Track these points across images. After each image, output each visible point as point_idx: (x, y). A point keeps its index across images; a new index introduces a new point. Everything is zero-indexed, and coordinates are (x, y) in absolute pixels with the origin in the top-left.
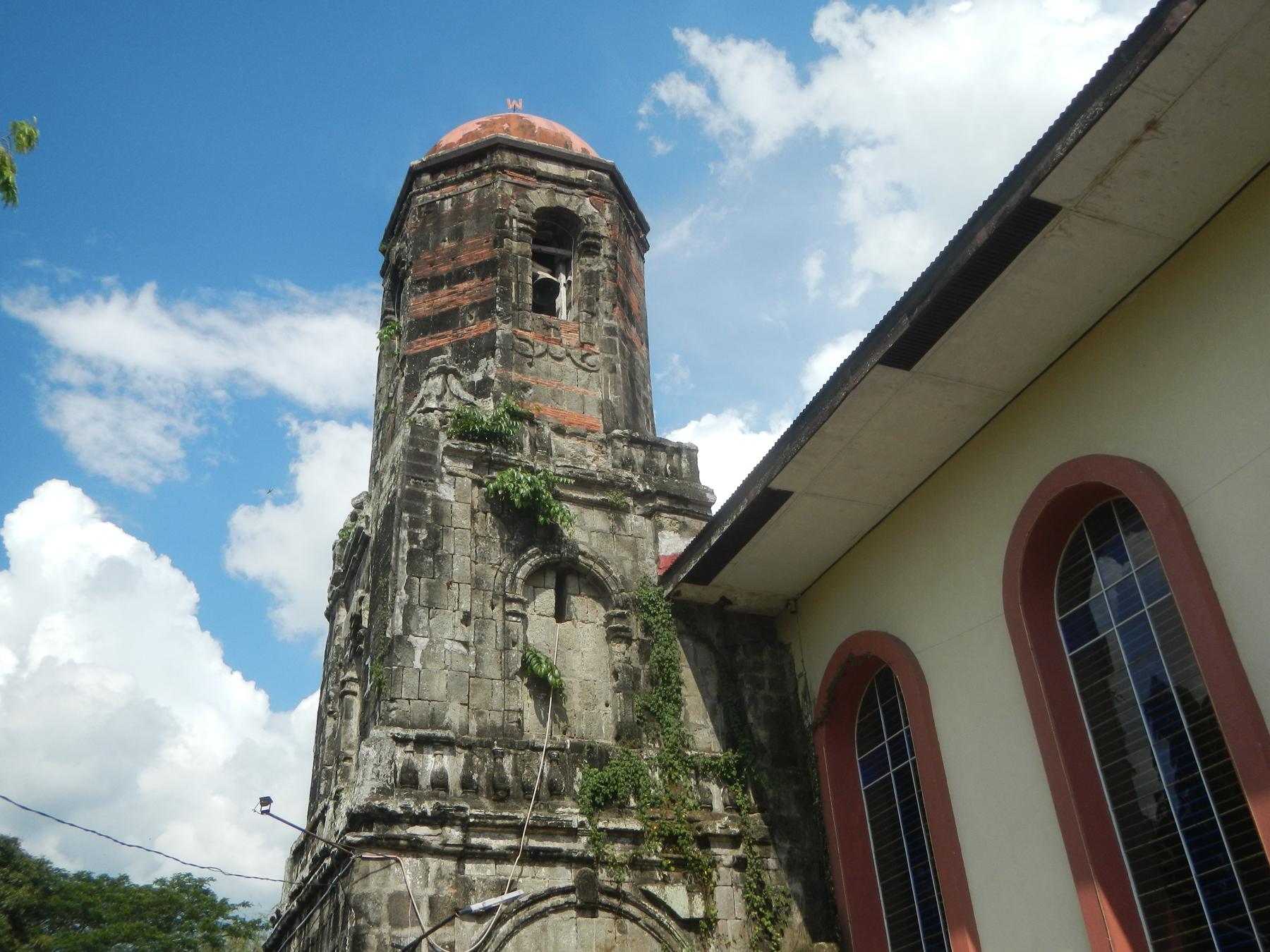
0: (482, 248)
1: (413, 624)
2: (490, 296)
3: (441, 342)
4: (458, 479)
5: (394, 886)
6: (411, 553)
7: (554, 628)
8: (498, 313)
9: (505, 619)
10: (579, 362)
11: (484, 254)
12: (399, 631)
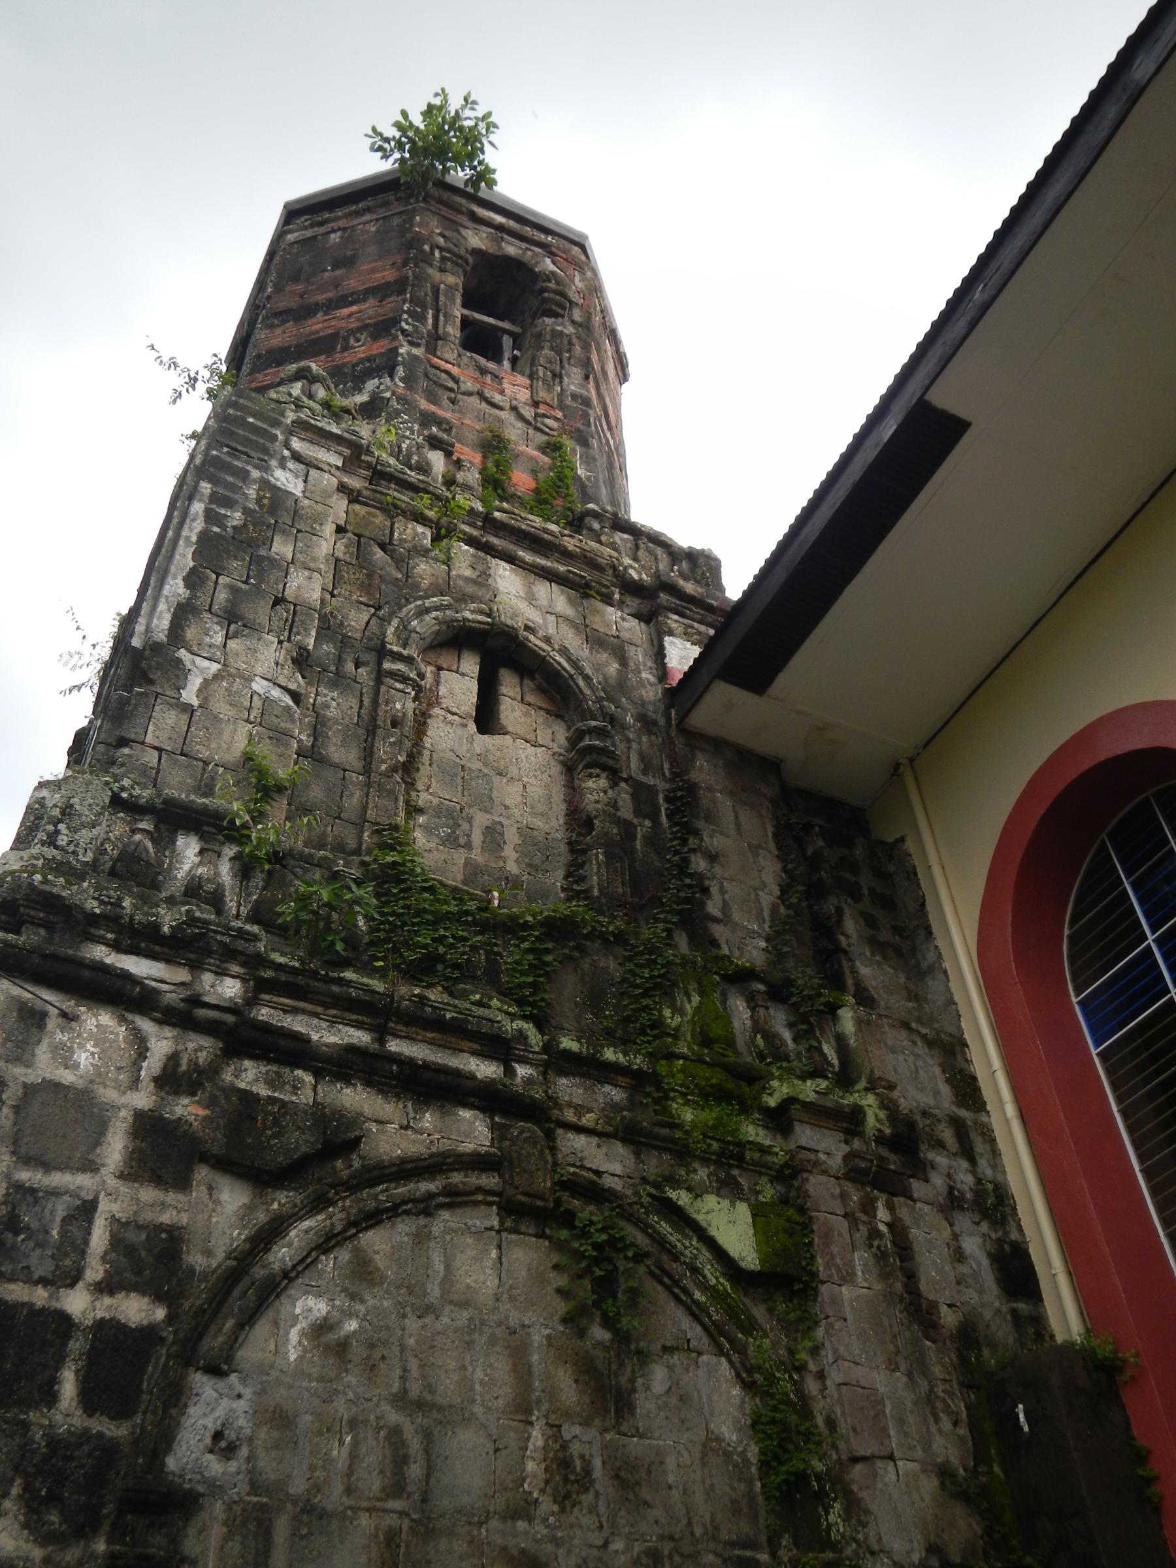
0: (384, 270)
1: (190, 633)
2: (391, 315)
4: (313, 473)
5: (44, 1066)
6: (204, 536)
7: (471, 740)
8: (403, 331)
9: (379, 682)
10: (531, 419)
11: (389, 275)
12: (161, 637)
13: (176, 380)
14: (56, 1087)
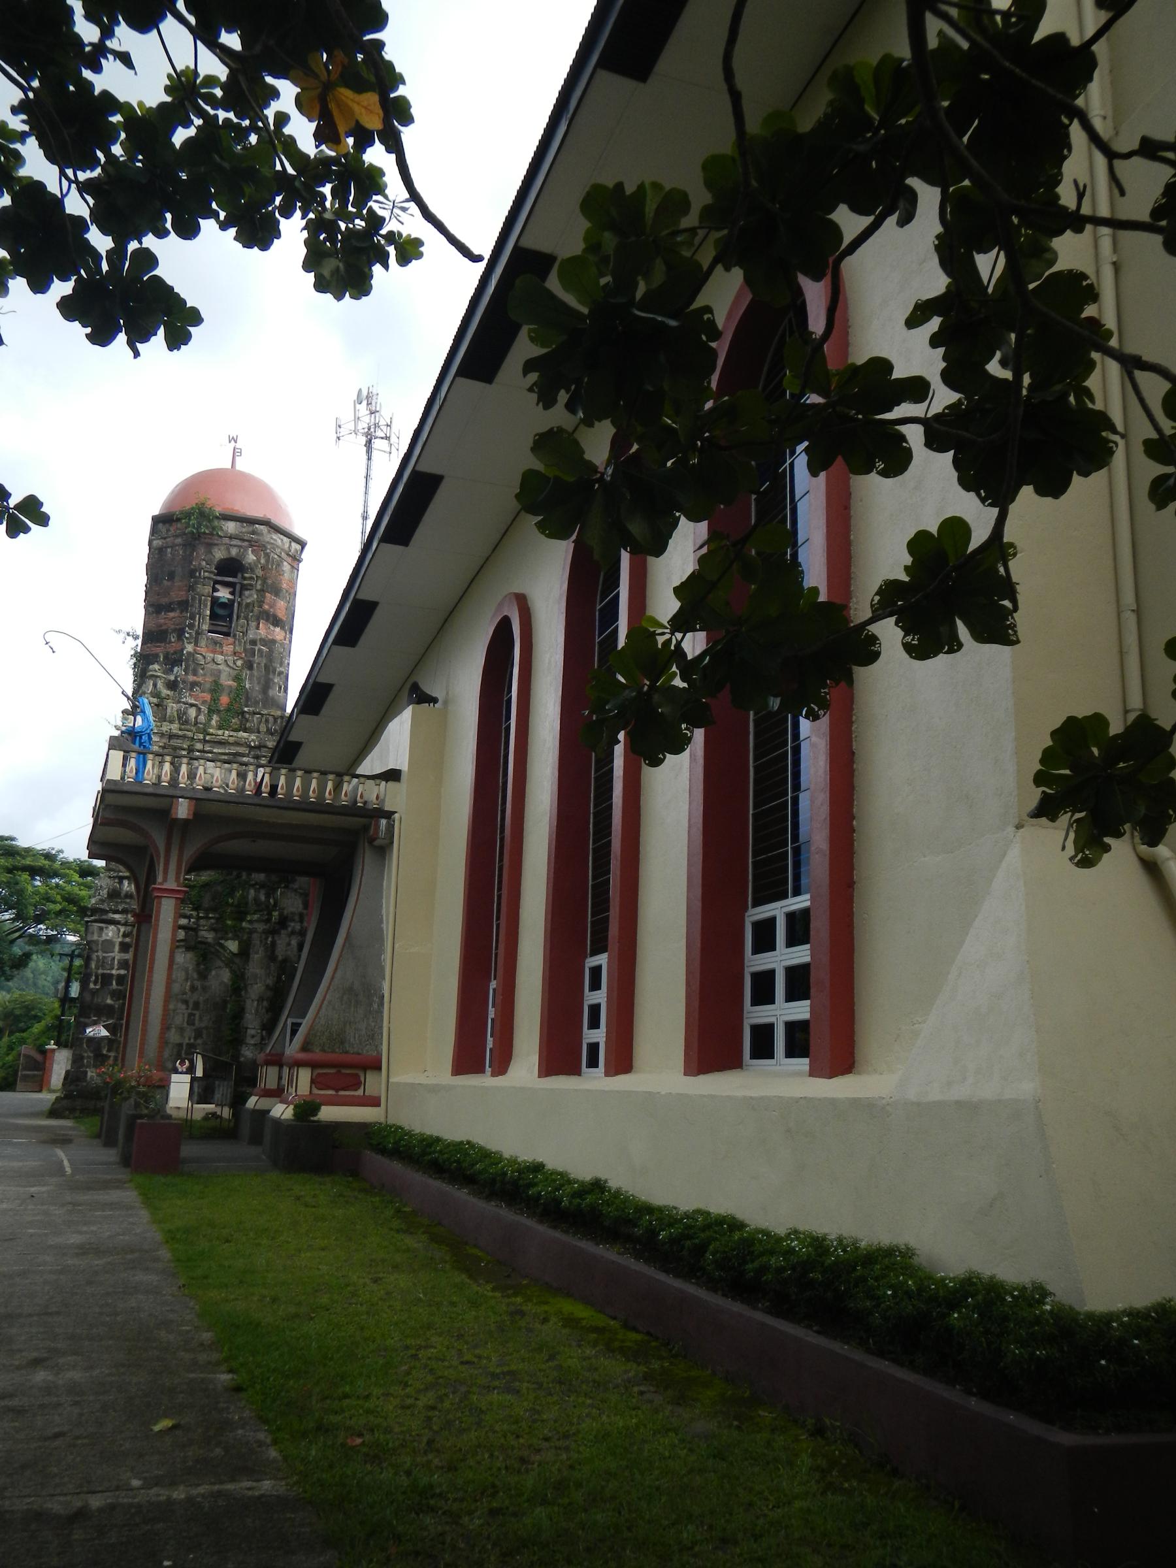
3: (158, 650)
5: (104, 937)
13: (122, 635)
14: (106, 940)
